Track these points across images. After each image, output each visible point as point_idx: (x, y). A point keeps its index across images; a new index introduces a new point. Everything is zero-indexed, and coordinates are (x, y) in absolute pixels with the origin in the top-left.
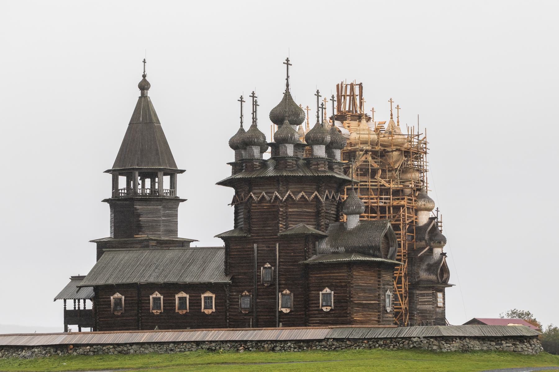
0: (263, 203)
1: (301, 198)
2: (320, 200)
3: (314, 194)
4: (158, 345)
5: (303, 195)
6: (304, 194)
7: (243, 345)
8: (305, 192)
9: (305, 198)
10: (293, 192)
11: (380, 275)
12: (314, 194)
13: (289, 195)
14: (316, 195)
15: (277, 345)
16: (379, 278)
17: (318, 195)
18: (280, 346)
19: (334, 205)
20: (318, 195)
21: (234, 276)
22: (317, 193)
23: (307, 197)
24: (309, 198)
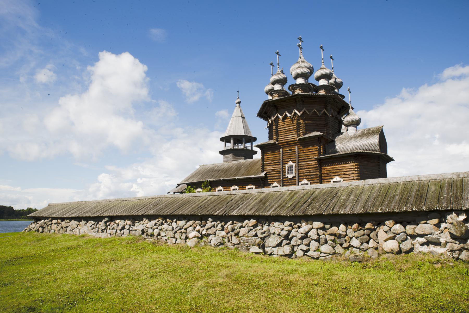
0: (286, 119)
1: (313, 114)
2: (327, 116)
3: (323, 111)
4: (92, 222)
5: (315, 112)
6: (315, 111)
7: (198, 227)
8: (317, 110)
9: (317, 114)
10: (308, 110)
11: (379, 165)
12: (323, 111)
13: (305, 111)
14: (324, 112)
15: (272, 230)
16: (379, 168)
17: (326, 111)
18: (279, 235)
19: (337, 122)
20: (326, 111)
21: (267, 173)
22: (325, 110)
23: (318, 113)
24: (319, 114)
